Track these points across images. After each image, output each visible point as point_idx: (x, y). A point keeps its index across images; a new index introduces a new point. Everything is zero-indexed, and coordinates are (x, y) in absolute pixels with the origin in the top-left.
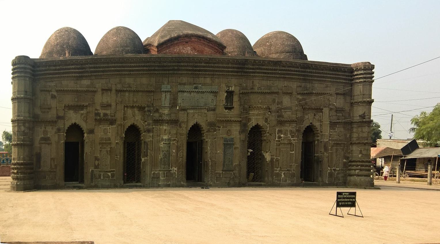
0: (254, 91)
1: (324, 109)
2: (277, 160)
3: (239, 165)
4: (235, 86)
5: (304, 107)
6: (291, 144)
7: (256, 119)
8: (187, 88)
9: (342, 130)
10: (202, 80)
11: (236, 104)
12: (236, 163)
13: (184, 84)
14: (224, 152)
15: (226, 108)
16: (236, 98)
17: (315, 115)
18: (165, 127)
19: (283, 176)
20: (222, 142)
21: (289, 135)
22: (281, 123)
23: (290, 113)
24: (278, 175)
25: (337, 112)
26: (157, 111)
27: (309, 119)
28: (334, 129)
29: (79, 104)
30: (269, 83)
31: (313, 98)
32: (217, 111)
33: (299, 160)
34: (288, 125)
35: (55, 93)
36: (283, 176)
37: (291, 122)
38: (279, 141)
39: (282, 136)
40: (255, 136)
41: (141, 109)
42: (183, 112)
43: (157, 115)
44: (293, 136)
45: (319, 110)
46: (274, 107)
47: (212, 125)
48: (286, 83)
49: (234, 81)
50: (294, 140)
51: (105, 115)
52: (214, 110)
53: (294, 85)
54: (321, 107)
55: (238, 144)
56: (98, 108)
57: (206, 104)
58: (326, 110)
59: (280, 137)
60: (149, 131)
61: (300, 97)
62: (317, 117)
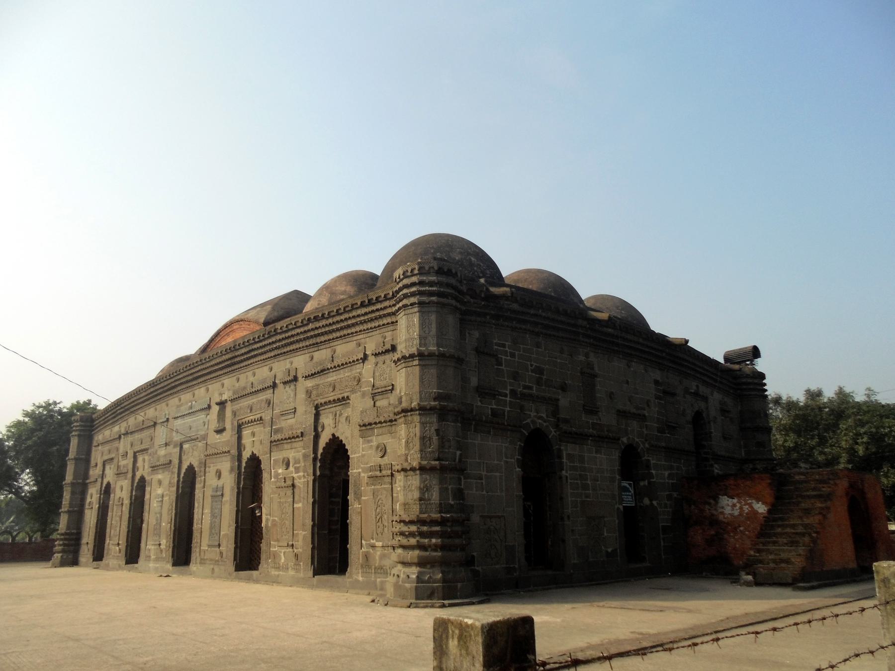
1: (352, 397)
5: (316, 402)
6: (293, 486)
7: (254, 442)
19: (283, 561)
21: (291, 468)
24: (275, 556)
25: (377, 398)
28: (369, 442)
31: (332, 377)
33: (309, 523)
34: (289, 446)
39: (280, 471)
40: (251, 477)
44: (297, 470)
50: (300, 478)
53: (300, 362)
54: (345, 395)
58: (355, 399)
59: (277, 475)
61: (310, 383)
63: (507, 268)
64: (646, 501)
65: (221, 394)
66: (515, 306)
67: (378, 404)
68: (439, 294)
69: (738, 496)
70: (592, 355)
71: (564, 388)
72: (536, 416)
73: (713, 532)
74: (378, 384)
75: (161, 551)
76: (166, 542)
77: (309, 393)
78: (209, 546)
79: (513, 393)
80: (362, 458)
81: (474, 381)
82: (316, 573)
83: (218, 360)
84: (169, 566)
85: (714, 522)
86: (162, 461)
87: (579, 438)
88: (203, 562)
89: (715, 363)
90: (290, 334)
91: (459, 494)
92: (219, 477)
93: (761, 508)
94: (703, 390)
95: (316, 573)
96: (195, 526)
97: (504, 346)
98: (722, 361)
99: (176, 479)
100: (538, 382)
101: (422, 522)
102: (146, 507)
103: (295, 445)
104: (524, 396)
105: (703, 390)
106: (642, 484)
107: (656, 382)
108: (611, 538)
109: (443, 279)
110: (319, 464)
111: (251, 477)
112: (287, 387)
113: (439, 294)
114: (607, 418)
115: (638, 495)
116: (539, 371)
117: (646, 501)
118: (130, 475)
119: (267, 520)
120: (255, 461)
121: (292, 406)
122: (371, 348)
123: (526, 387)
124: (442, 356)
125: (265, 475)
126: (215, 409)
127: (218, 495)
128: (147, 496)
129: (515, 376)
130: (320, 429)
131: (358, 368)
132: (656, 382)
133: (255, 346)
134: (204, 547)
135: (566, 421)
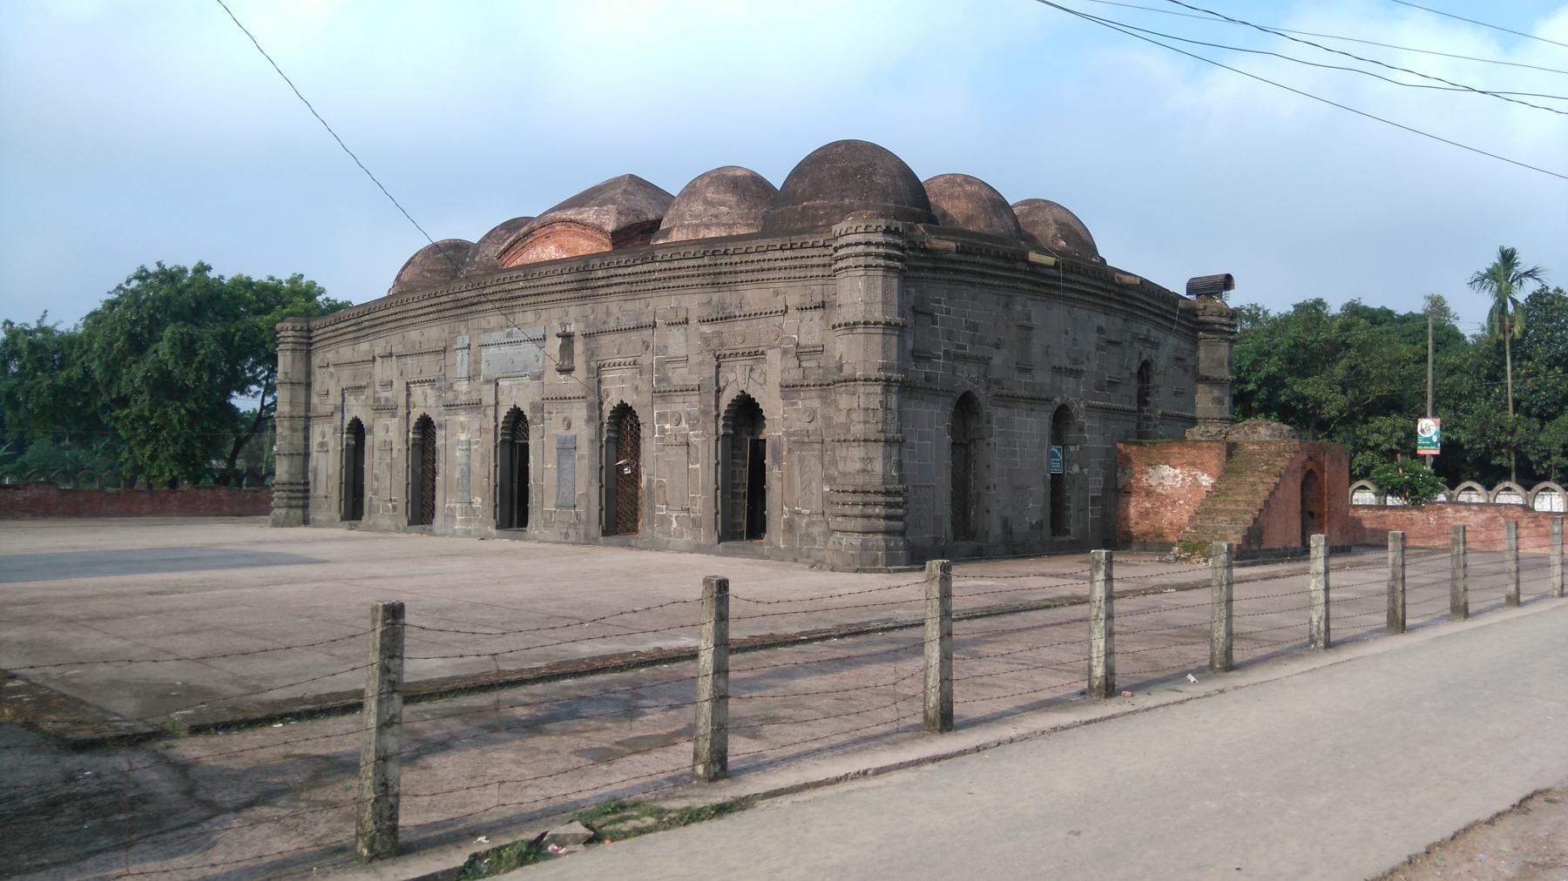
0: (606, 327)
1: (770, 353)
2: (661, 486)
3: (587, 495)
4: (576, 320)
8: (498, 336)
9: (816, 403)
10: (519, 317)
11: (579, 362)
12: (581, 489)
13: (492, 330)
14: (559, 464)
15: (561, 371)
16: (579, 347)
17: (751, 370)
18: (462, 418)
19: (675, 524)
20: (555, 445)
21: (684, 424)
22: (663, 395)
23: (685, 371)
24: (664, 521)
26: (451, 387)
27: (736, 381)
29: (357, 383)
30: (638, 305)
31: (740, 326)
32: (546, 380)
35: (331, 369)
36: (675, 524)
37: (686, 390)
38: (662, 439)
39: (668, 426)
40: (622, 428)
41: (432, 382)
42: (488, 387)
43: (450, 395)
44: (693, 427)
45: (757, 355)
46: (646, 359)
47: (538, 408)
48: (674, 302)
49: (574, 310)
51: (387, 399)
52: (539, 377)
53: (693, 302)
55: (585, 448)
56: (378, 388)
57: (526, 367)
58: (773, 356)
59: (663, 431)
60: (440, 426)
61: (707, 329)
62: (756, 375)
64: (1076, 469)
65: (563, 325)
67: (804, 364)
68: (887, 257)
69: (1182, 465)
70: (1030, 303)
71: (997, 347)
72: (967, 377)
73: (1148, 505)
74: (803, 343)
75: (474, 511)
76: (482, 501)
77: (706, 339)
78: (558, 506)
80: (781, 421)
81: (910, 344)
82: (720, 540)
83: (555, 280)
84: (492, 530)
85: (1149, 493)
86: (463, 399)
87: (1008, 400)
88: (547, 524)
89: (1172, 298)
90: (676, 264)
91: (900, 465)
92: (569, 426)
93: (1206, 481)
94: (1155, 334)
95: (720, 540)
96: (531, 481)
97: (939, 302)
98: (1183, 293)
99: (492, 425)
100: (972, 343)
101: (888, 493)
102: (440, 457)
103: (688, 399)
104: (957, 357)
105: (1155, 334)
106: (1072, 448)
107: (1100, 330)
108: (1035, 508)
109: (890, 239)
110: (721, 423)
111: (622, 428)
112: (675, 329)
113: (887, 257)
114: (1042, 377)
115: (1066, 462)
116: (975, 327)
117: (1076, 469)
118: (402, 411)
119: (649, 481)
120: (624, 412)
121: (683, 353)
122: (794, 300)
123: (959, 347)
124: (888, 324)
125: (645, 432)
126: (555, 344)
127: (566, 448)
128: (439, 442)
129: (950, 336)
130: (722, 384)
131: (778, 320)
132: (1100, 330)
133: (621, 271)
134: (550, 506)
135: (998, 382)
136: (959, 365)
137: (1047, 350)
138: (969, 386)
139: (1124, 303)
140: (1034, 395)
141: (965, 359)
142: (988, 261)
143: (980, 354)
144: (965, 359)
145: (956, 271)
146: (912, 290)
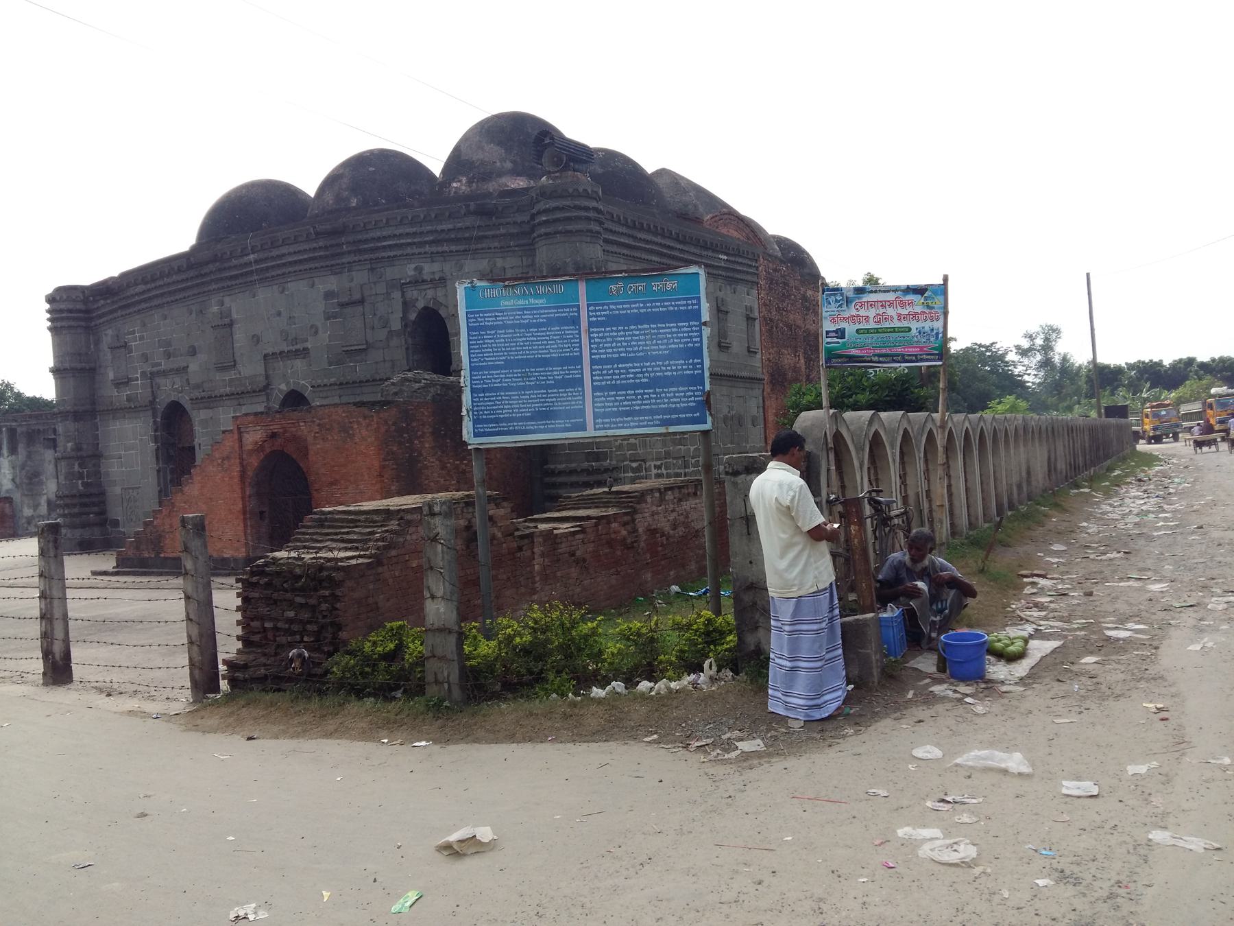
63: (310, 186)
66: (141, 288)
70: (227, 299)
72: (169, 390)
79: (143, 373)
107: (329, 295)
129: (145, 357)
135: (197, 386)
136: (161, 381)
137: (256, 339)
138: (173, 397)
139: (360, 251)
140: (239, 390)
141: (165, 373)
142: (175, 278)
143: (175, 366)
144: (165, 373)
145: (145, 300)
146: (110, 332)
